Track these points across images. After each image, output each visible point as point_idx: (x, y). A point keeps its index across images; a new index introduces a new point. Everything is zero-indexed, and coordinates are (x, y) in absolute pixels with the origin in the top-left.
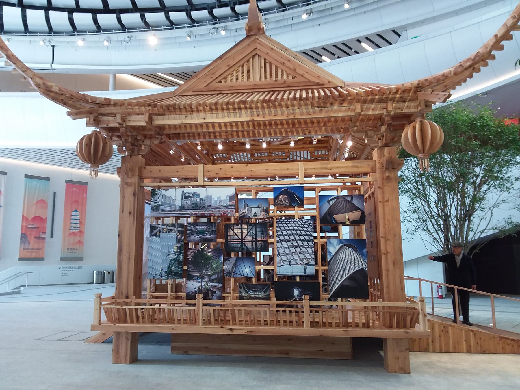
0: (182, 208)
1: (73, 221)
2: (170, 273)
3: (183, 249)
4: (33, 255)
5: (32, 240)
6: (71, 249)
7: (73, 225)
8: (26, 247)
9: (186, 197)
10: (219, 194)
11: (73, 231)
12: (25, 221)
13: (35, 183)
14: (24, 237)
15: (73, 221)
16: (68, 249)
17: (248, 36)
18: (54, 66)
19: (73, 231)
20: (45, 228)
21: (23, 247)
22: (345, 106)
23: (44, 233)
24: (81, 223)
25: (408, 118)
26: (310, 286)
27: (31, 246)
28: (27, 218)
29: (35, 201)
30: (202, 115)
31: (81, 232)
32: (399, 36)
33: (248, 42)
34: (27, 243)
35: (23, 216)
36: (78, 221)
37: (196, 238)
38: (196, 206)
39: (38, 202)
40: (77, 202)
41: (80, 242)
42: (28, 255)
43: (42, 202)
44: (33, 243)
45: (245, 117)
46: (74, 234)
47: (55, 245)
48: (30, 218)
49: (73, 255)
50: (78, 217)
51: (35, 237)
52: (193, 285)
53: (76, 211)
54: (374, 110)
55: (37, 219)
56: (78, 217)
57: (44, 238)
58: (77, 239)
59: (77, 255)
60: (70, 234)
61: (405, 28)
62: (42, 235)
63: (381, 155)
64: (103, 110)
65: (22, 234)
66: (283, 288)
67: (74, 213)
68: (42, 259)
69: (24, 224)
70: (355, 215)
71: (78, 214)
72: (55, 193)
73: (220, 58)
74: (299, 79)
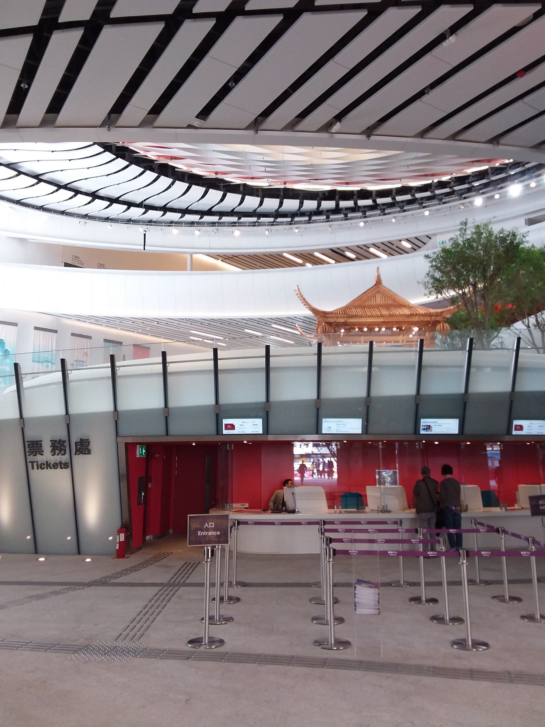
17: (375, 285)
22: (417, 317)
25: (439, 322)
30: (365, 318)
32: (430, 238)
33: (375, 287)
45: (381, 320)
54: (427, 319)
61: (435, 235)
63: (429, 334)
64: (327, 316)
73: (364, 293)
74: (396, 303)
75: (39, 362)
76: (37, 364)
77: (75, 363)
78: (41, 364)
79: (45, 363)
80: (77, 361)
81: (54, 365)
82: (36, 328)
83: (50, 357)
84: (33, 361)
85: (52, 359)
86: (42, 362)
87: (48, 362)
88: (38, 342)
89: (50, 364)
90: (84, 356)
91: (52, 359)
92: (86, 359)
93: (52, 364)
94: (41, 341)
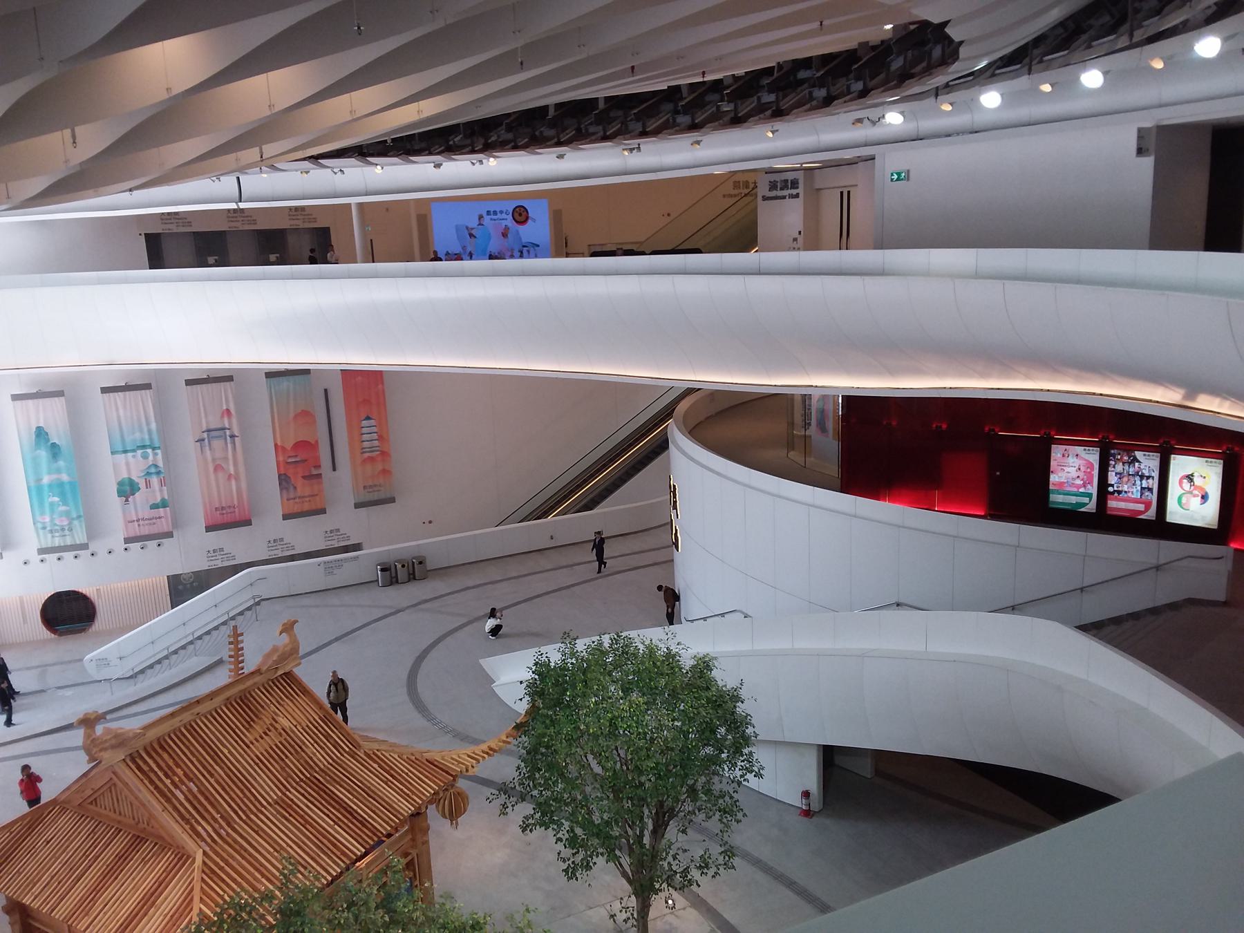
1: (365, 437)
4: (306, 507)
5: (299, 482)
7: (366, 444)
8: (292, 496)
12: (280, 453)
13: (285, 383)
14: (284, 480)
15: (365, 437)
18: (242, 205)
20: (317, 459)
21: (285, 497)
23: (319, 467)
24: (381, 438)
27: (299, 493)
28: (283, 449)
29: (292, 415)
31: (384, 454)
34: (292, 489)
35: (276, 445)
36: (375, 436)
39: (296, 417)
40: (367, 402)
41: (385, 472)
42: (296, 509)
43: (305, 416)
44: (303, 488)
46: (372, 459)
47: (342, 483)
48: (289, 444)
49: (375, 496)
50: (374, 429)
51: (304, 477)
53: (368, 418)
55: (301, 445)
56: (374, 429)
57: (319, 476)
58: (379, 467)
59: (382, 496)
60: (364, 461)
62: (315, 472)
65: (280, 476)
67: (365, 423)
68: (323, 511)
69: (281, 459)
71: (372, 422)
75: (125, 452)
76: (121, 458)
77: (205, 435)
78: (130, 455)
79: (140, 452)
80: (209, 431)
81: (159, 451)
82: (105, 390)
83: (147, 437)
84: (112, 453)
85: (151, 439)
86: (134, 451)
87: (144, 447)
88: (115, 414)
89: (149, 451)
90: (222, 416)
91: (151, 439)
92: (230, 423)
93: (154, 449)
94: (121, 412)
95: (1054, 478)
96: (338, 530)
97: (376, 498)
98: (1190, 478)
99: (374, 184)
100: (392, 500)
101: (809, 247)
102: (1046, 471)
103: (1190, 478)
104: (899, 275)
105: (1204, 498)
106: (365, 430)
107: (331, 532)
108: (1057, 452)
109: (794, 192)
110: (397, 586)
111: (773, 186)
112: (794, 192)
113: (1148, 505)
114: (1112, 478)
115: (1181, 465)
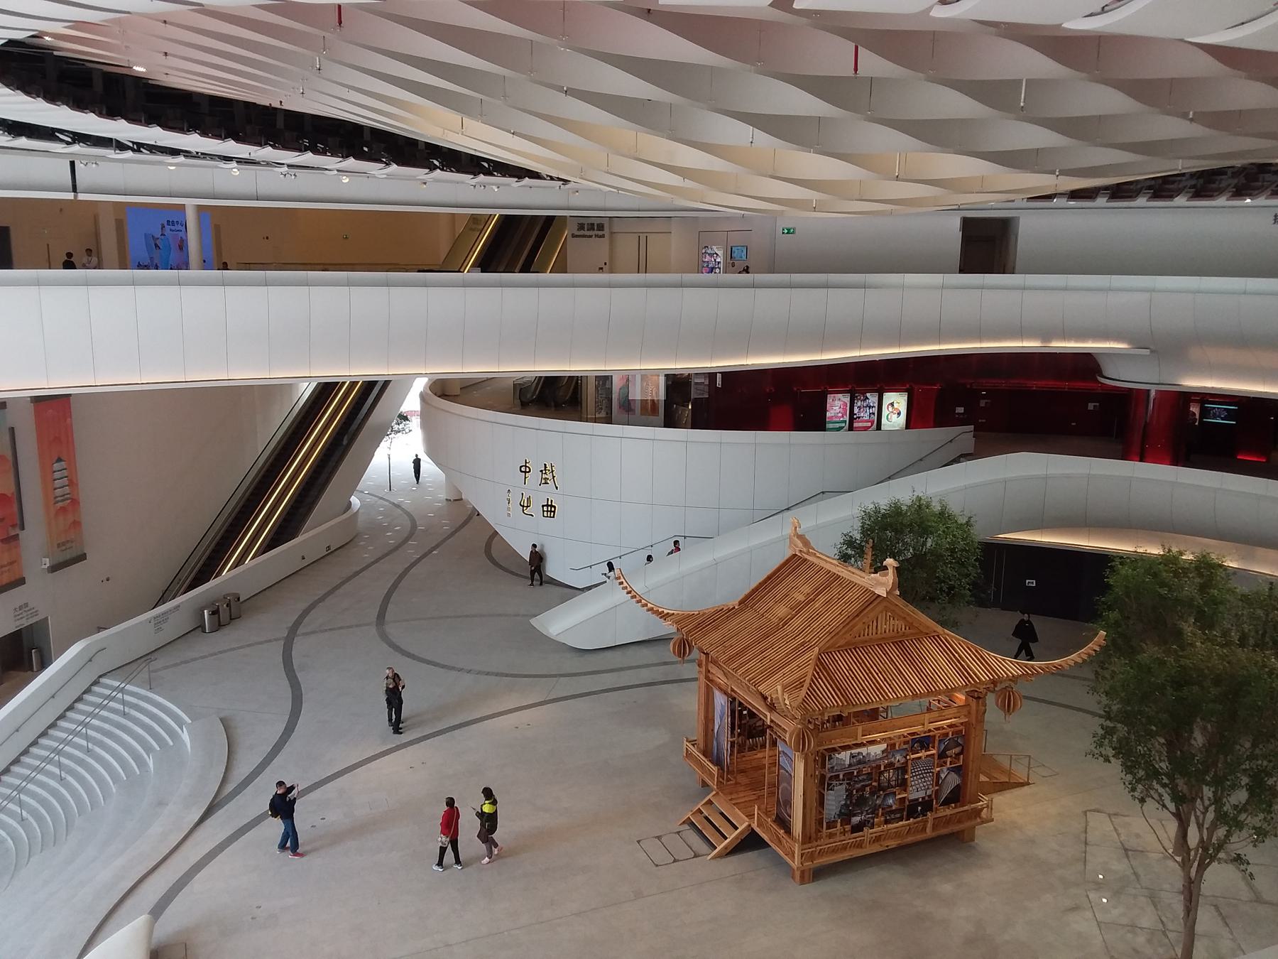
0: (850, 765)
2: (841, 814)
3: (850, 796)
6: (64, 544)
7: (58, 492)
9: (852, 756)
10: (876, 750)
11: (60, 504)
16: (59, 546)
19: (60, 504)
26: (927, 805)
31: (75, 502)
37: (858, 786)
38: (860, 762)
41: (76, 524)
46: (63, 509)
49: (68, 555)
50: (65, 473)
52: (856, 820)
53: (59, 460)
56: (65, 473)
66: (913, 809)
67: (57, 466)
70: (958, 750)
72: (12, 430)
95: (828, 414)
96: (26, 605)
97: (68, 557)
98: (892, 404)
99: (264, 189)
100: (82, 557)
101: (611, 272)
102: (824, 410)
103: (892, 404)
104: (876, 288)
105: (899, 414)
106: (57, 475)
107: (20, 608)
108: (830, 398)
109: (600, 233)
110: (225, 631)
111: (581, 227)
112: (600, 233)
113: (872, 423)
114: (856, 410)
115: (889, 397)
